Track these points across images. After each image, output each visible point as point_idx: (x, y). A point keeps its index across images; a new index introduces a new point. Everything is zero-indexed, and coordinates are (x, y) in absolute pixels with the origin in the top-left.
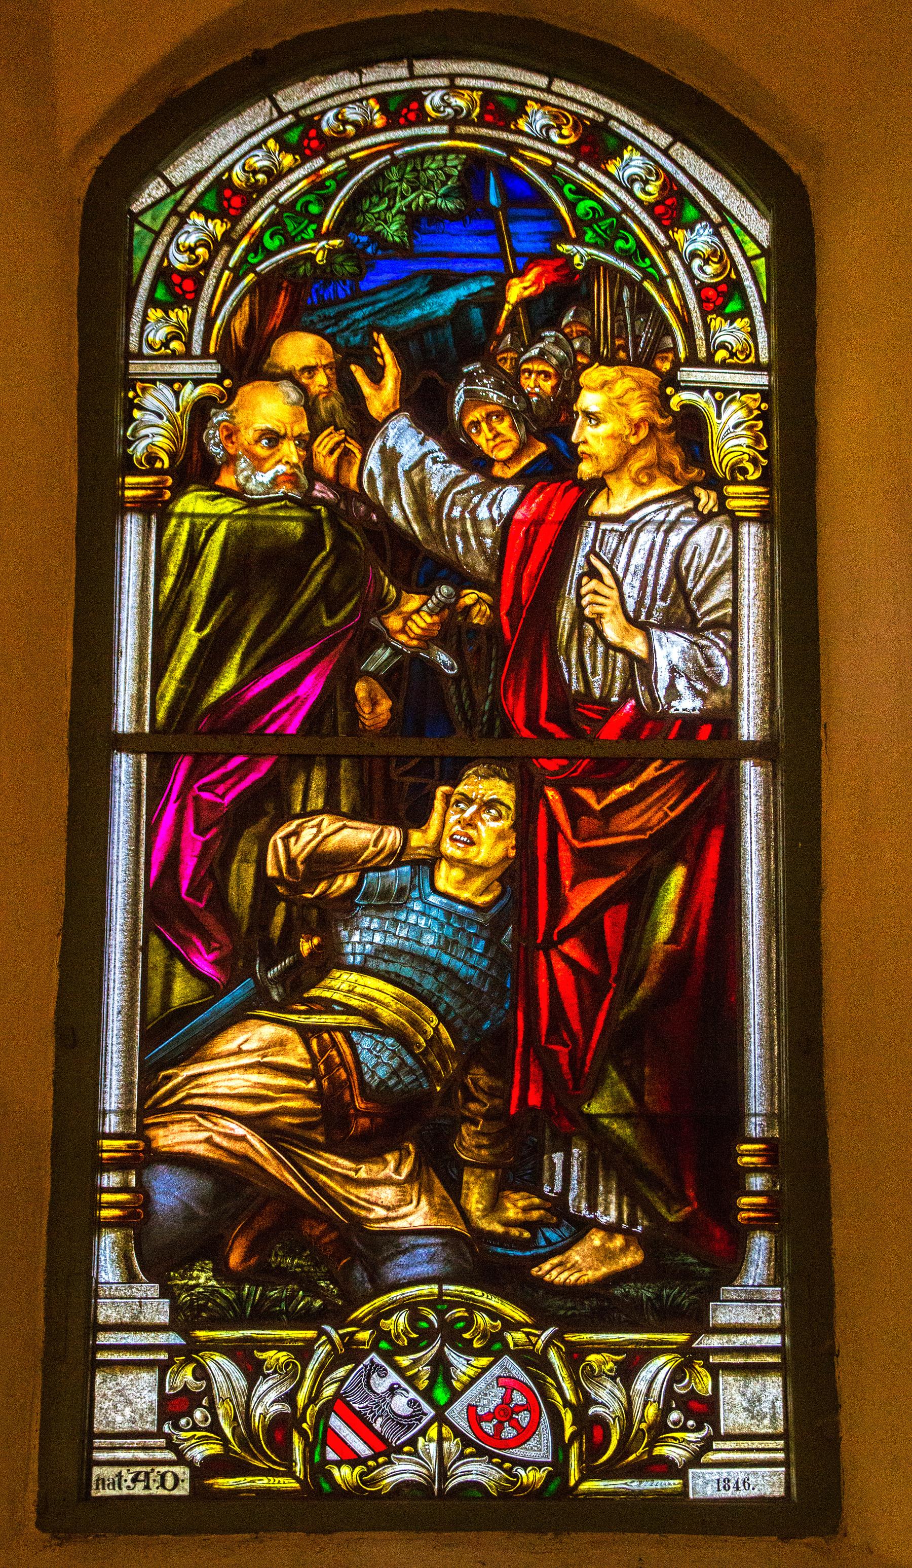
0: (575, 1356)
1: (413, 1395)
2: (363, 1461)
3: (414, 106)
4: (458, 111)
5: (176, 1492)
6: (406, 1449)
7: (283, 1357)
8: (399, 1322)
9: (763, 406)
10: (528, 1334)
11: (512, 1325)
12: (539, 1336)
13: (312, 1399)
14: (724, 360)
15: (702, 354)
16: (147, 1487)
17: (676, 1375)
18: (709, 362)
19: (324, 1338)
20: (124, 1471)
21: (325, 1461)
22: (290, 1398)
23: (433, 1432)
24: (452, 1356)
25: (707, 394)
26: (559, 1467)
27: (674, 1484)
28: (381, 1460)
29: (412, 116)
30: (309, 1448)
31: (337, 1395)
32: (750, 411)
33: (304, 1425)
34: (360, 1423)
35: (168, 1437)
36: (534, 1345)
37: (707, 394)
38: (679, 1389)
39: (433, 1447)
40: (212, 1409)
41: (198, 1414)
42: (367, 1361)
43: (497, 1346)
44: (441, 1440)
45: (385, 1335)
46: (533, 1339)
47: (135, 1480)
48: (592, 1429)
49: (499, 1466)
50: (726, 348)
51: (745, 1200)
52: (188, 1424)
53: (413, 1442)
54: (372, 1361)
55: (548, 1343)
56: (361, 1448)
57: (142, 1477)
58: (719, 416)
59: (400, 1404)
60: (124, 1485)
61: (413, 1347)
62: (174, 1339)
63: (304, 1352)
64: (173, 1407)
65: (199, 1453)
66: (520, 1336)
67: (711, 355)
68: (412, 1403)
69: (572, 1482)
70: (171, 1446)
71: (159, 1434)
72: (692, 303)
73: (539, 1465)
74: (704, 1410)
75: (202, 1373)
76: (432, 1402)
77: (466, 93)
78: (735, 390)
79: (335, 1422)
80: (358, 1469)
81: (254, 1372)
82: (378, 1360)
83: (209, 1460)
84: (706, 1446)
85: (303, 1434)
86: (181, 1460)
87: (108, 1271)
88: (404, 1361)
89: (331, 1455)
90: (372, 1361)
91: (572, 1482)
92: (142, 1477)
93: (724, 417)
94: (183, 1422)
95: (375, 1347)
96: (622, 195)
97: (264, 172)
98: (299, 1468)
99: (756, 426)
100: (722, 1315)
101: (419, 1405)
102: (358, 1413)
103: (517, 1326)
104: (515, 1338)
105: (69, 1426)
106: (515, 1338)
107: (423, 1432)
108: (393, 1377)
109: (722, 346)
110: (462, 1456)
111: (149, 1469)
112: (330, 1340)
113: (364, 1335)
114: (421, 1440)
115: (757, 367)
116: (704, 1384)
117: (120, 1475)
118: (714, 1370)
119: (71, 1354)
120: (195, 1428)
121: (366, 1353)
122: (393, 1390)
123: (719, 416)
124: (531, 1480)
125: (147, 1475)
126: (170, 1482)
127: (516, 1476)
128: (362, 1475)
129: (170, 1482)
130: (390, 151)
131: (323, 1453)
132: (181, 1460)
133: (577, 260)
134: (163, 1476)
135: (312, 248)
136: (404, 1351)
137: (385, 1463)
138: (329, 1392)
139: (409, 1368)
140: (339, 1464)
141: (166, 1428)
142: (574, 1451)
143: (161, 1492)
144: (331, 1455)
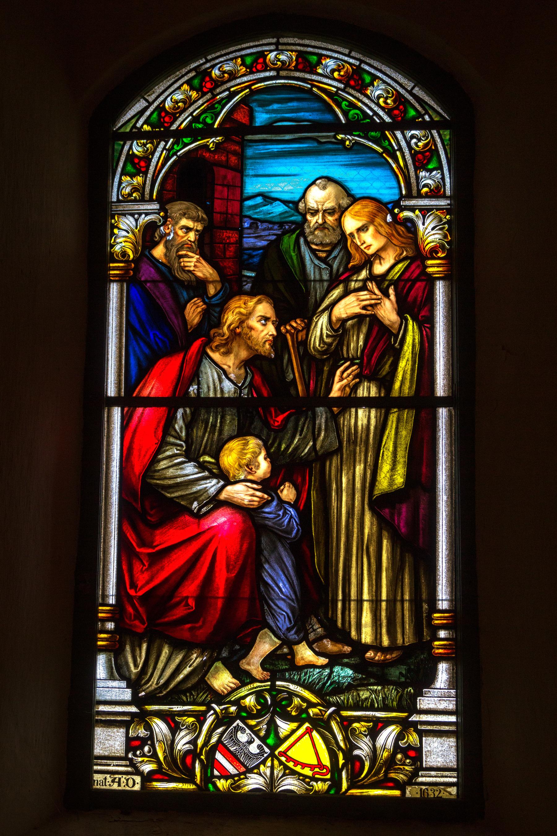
0: (346, 724)
2: (232, 776)
3: (261, 60)
4: (283, 62)
6: (255, 771)
7: (191, 720)
8: (250, 701)
9: (448, 217)
11: (311, 705)
12: (326, 712)
14: (426, 193)
15: (414, 192)
16: (119, 785)
17: (400, 737)
18: (420, 196)
19: (212, 712)
20: (108, 776)
21: (213, 776)
22: (194, 742)
23: (269, 763)
24: (279, 722)
25: (417, 212)
26: (336, 783)
27: (397, 793)
28: (242, 777)
29: (259, 67)
30: (204, 768)
31: (219, 741)
32: (441, 220)
33: (202, 757)
35: (131, 760)
36: (323, 716)
37: (417, 212)
38: (401, 743)
39: (268, 772)
40: (153, 746)
41: (146, 749)
42: (235, 725)
43: (304, 716)
44: (272, 768)
46: (323, 713)
47: (113, 781)
49: (303, 780)
50: (428, 187)
51: (437, 643)
52: (140, 753)
53: (257, 767)
54: (238, 724)
56: (232, 770)
57: (117, 780)
58: (423, 224)
60: (107, 784)
61: (259, 715)
62: (133, 709)
63: (201, 718)
64: (133, 745)
65: (147, 768)
66: (316, 710)
67: (419, 191)
68: (259, 747)
69: (343, 790)
70: (132, 764)
71: (126, 758)
72: (410, 161)
73: (324, 781)
75: (148, 728)
76: (268, 746)
77: (289, 53)
78: (432, 209)
79: (219, 756)
80: (229, 781)
81: (174, 728)
82: (241, 724)
83: (151, 772)
84: (415, 774)
85: (201, 761)
86: (138, 772)
87: (101, 671)
88: (253, 722)
89: (216, 773)
90: (238, 724)
91: (343, 790)
92: (117, 780)
93: (426, 224)
94: (138, 752)
95: (238, 716)
96: (373, 106)
97: (182, 102)
99: (444, 228)
100: (424, 703)
101: (263, 749)
103: (314, 705)
104: (312, 711)
105: (79, 756)
106: (312, 711)
107: (264, 762)
109: (426, 186)
110: (284, 775)
111: (120, 776)
112: (216, 712)
113: (233, 709)
114: (262, 767)
115: (444, 196)
116: (413, 738)
117: (105, 779)
119: (80, 714)
120: (144, 755)
121: (233, 720)
123: (423, 224)
124: (320, 788)
125: (120, 779)
126: (131, 782)
127: (312, 786)
128: (232, 784)
129: (131, 782)
130: (249, 87)
131: (212, 772)
132: (138, 772)
133: (347, 143)
134: (127, 780)
135: (208, 142)
136: (253, 717)
137: (243, 779)
138: (214, 740)
139: (256, 726)
140: (219, 778)
141: (130, 756)
142: (344, 774)
143: (127, 788)
144: (216, 773)
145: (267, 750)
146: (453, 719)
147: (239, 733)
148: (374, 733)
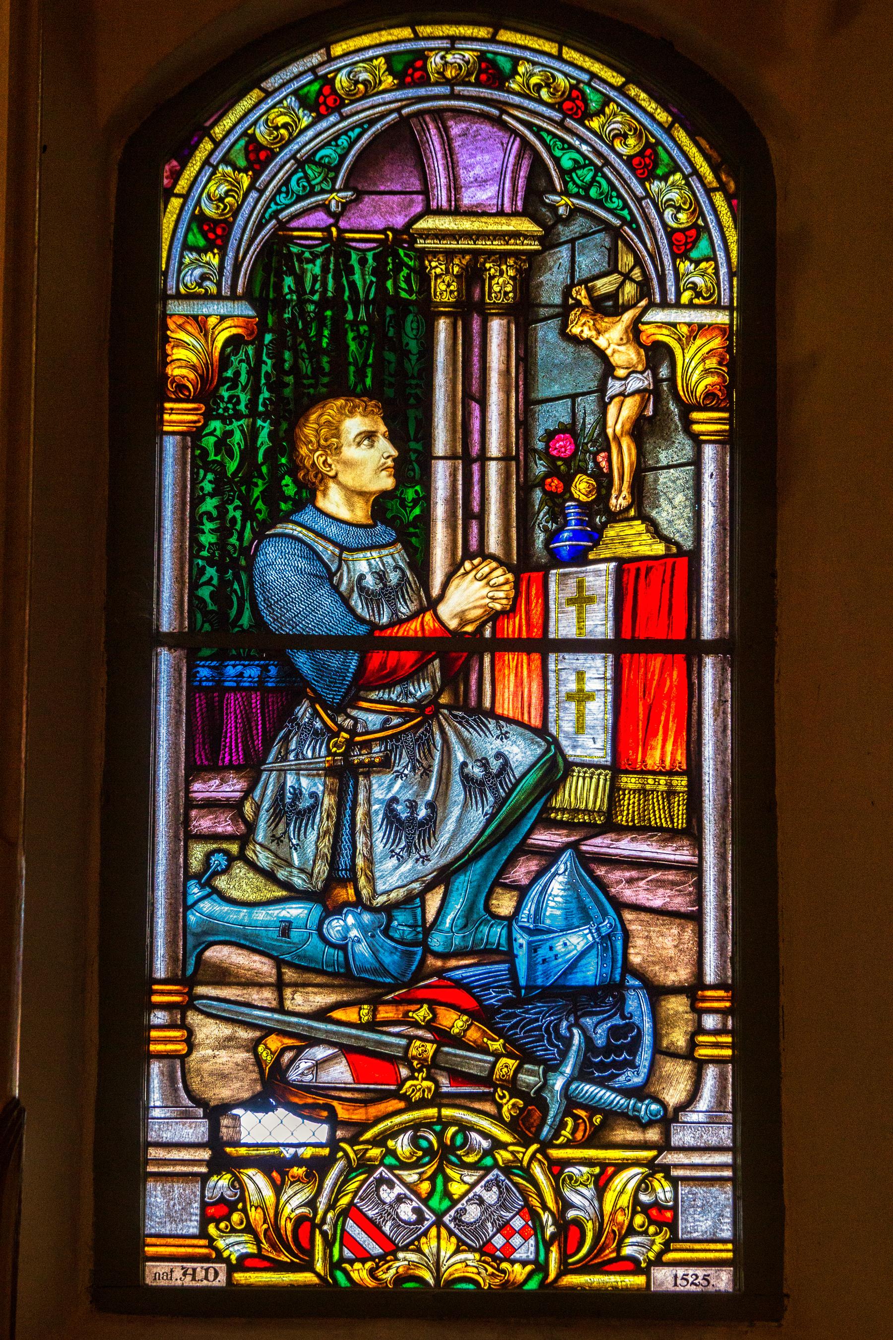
1: (416, 1203)
5: (216, 1283)
10: (512, 1153)
11: (498, 1145)
12: (524, 1154)
13: (331, 1206)
22: (312, 1203)
31: (351, 1204)
34: (372, 1227)
41: (236, 1217)
42: (376, 1175)
45: (393, 1153)
46: (520, 1156)
48: (568, 1231)
52: (227, 1227)
55: (533, 1157)
59: (406, 1212)
74: (664, 1217)
75: (238, 1184)
82: (387, 1174)
85: (324, 1234)
89: (347, 1253)
98: (319, 1267)
102: (371, 1220)
103: (504, 1146)
104: (503, 1156)
106: (503, 1156)
107: (425, 1234)
108: (399, 1189)
112: (346, 1155)
113: (375, 1152)
118: (674, 1182)
120: (233, 1230)
121: (376, 1168)
122: (400, 1199)
138: (344, 1201)
145: (428, 1215)
146: (727, 1158)
147: (385, 1187)
148: (601, 1185)
